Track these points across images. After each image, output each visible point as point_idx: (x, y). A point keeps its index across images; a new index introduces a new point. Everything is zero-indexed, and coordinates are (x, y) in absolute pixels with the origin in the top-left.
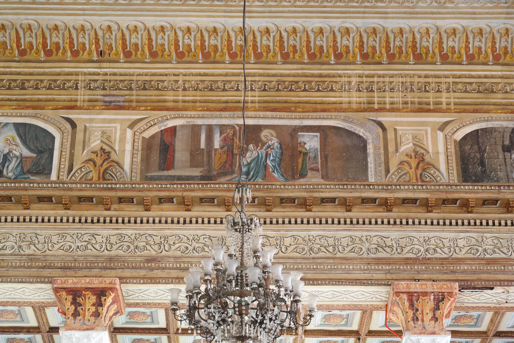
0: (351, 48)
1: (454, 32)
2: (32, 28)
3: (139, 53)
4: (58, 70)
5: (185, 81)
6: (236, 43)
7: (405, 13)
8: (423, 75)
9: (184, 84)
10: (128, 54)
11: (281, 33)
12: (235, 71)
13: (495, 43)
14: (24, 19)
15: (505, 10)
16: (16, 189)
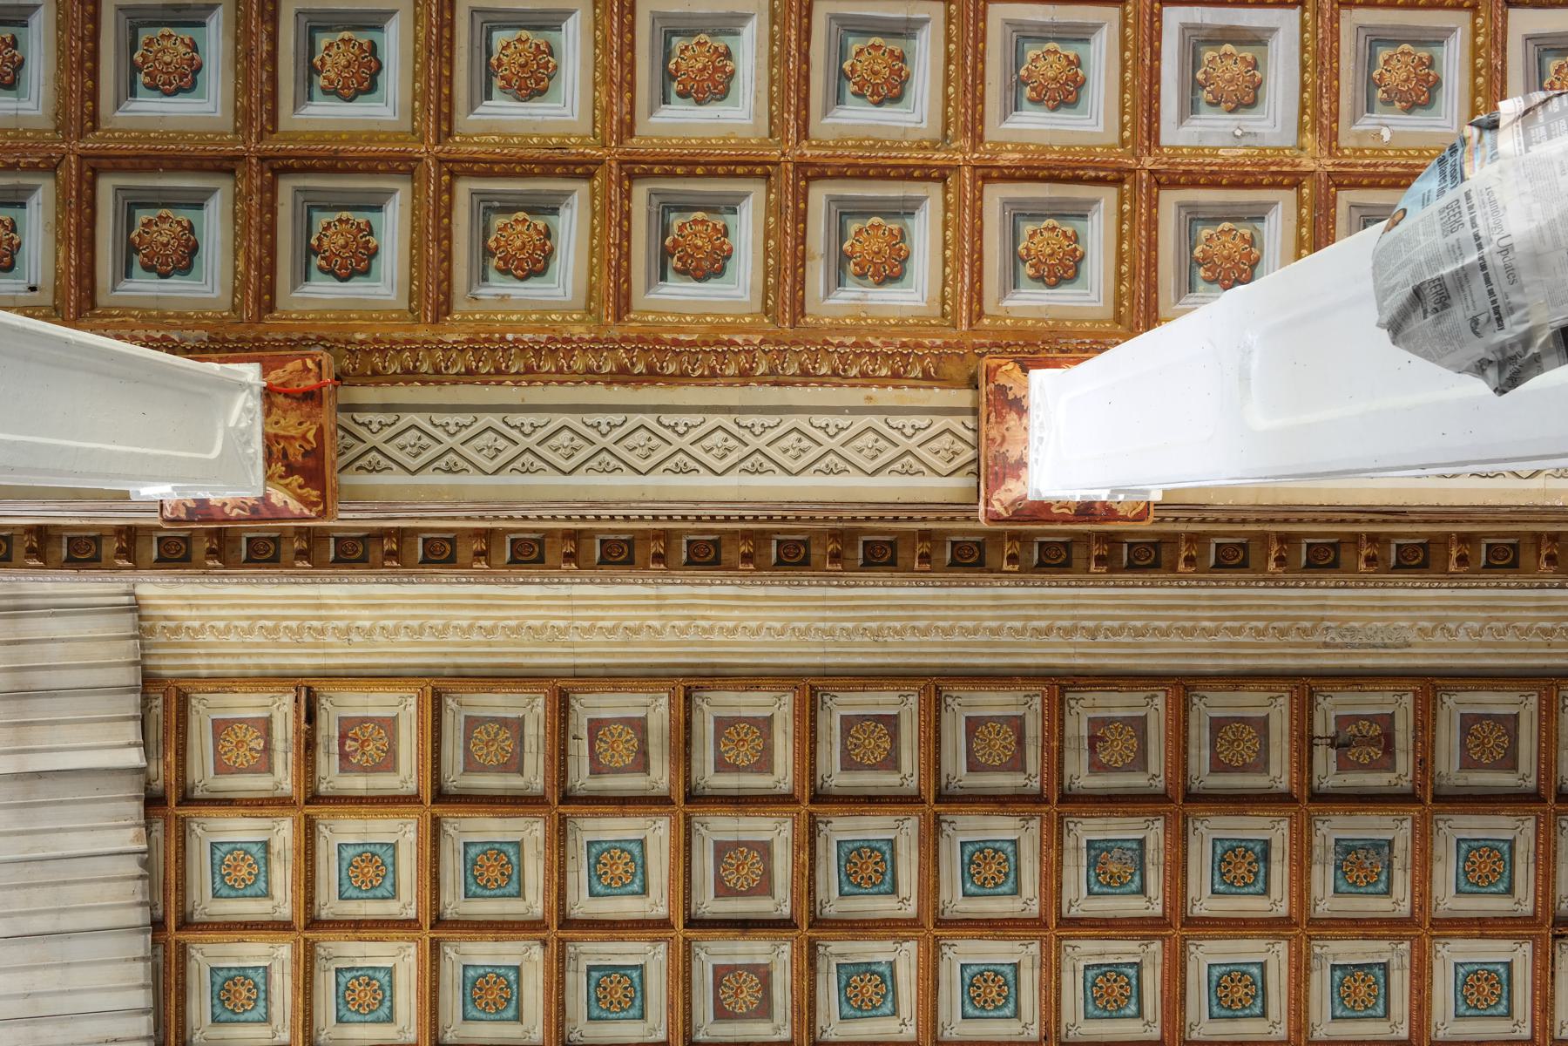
7: (1505, 608)
15: (1328, 613)
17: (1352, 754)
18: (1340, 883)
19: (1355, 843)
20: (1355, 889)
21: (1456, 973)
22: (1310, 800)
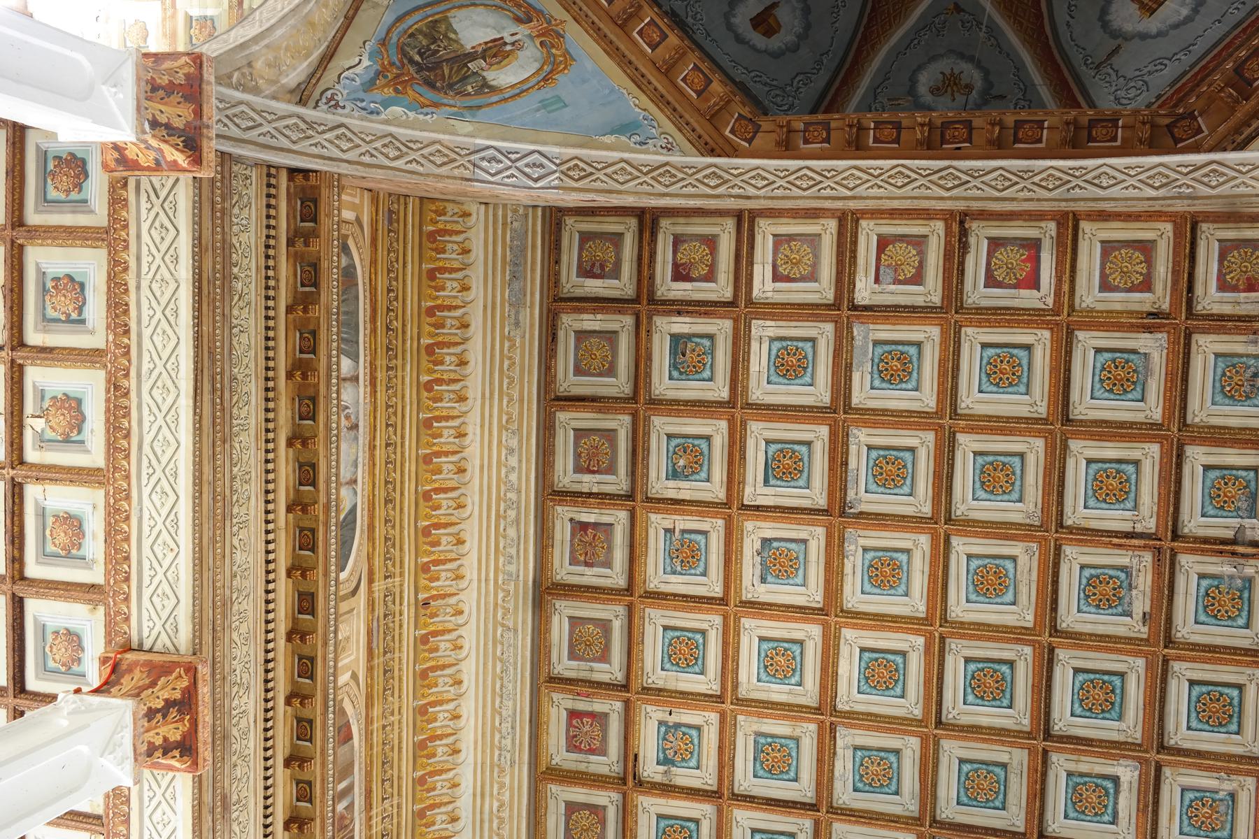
2: (460, 510)
3: (427, 654)
4: (406, 547)
5: (392, 724)
6: (437, 781)
10: (424, 640)
12: (404, 789)
14: (473, 499)
16: (326, 557)
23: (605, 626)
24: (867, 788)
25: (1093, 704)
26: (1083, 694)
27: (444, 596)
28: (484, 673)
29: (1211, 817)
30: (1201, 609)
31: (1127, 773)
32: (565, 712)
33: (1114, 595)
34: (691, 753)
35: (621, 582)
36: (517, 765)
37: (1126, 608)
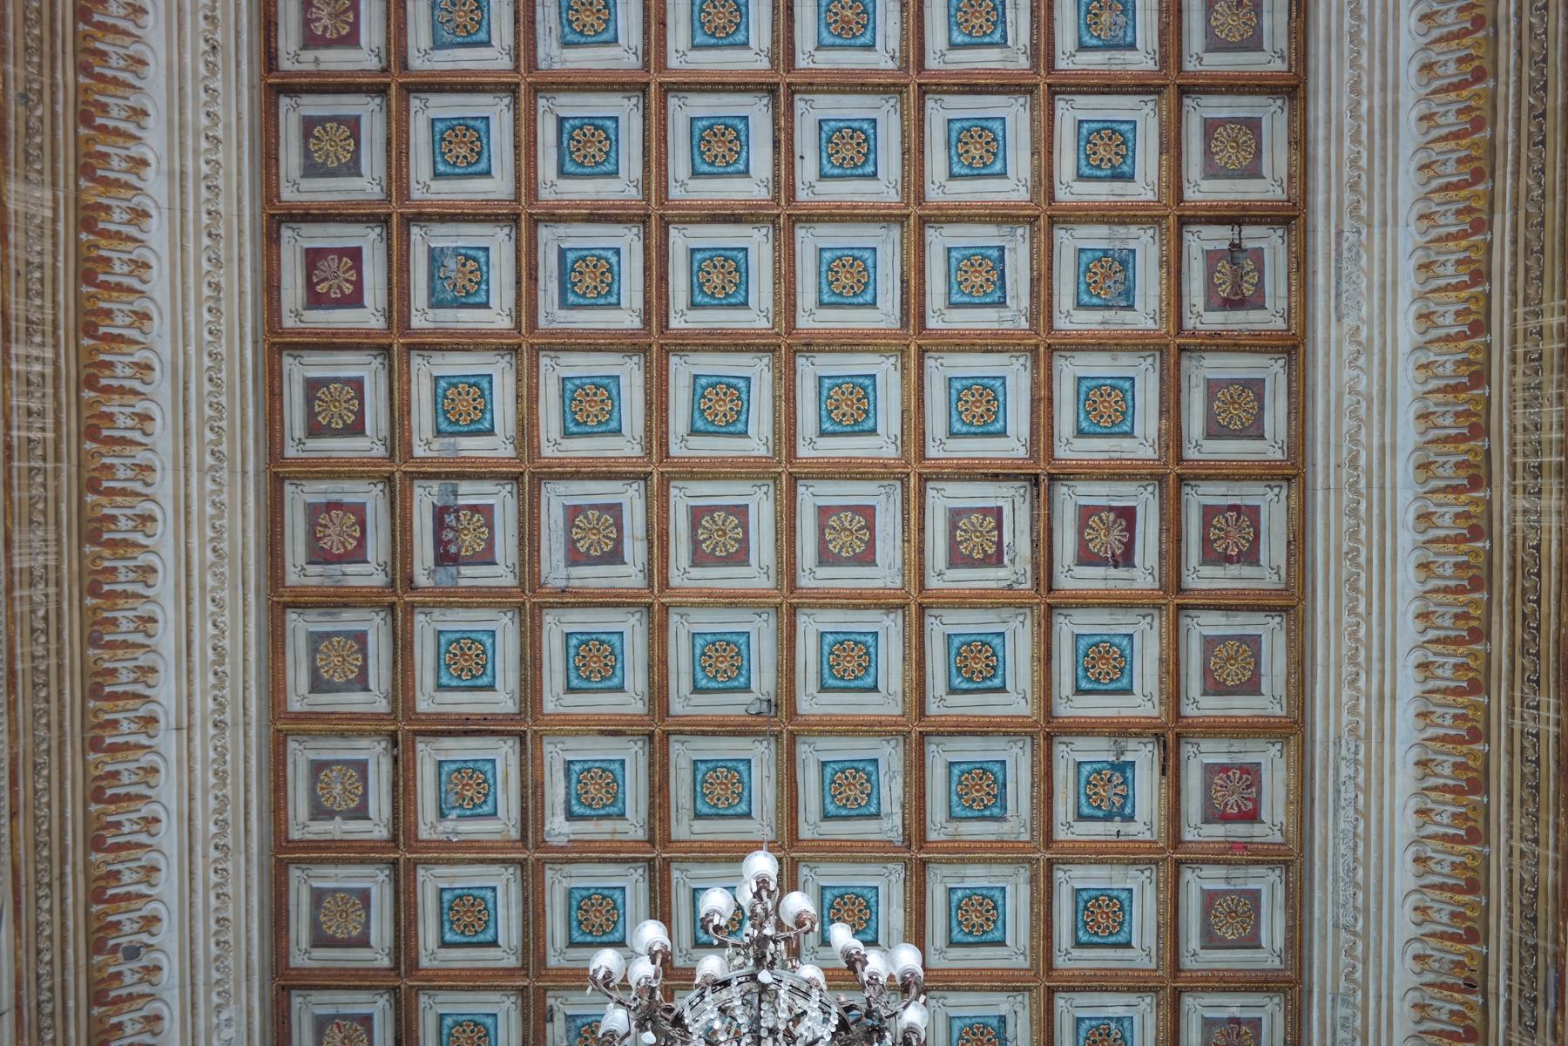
0: (1460, 510)
1: (1425, 316)
3: (1469, 913)
5: (1522, 838)
7: (1382, 413)
8: (1512, 367)
9: (1527, 840)
11: (1429, 642)
12: (1503, 735)
13: (1449, 234)
15: (1376, 231)
17: (1223, 266)
18: (1090, 255)
19: (1131, 270)
20: (1083, 271)
21: (995, 378)
22: (1180, 217)
23: (1211, 940)
24: (861, 766)
25: (601, 904)
26: (613, 915)
27: (1442, 986)
28: (1381, 868)
29: (464, 785)
30: (492, 1032)
31: (558, 827)
32: (1264, 817)
33: (586, 1039)
34: (1089, 783)
35: (1188, 1001)
36: (1331, 739)
37: (572, 1025)
